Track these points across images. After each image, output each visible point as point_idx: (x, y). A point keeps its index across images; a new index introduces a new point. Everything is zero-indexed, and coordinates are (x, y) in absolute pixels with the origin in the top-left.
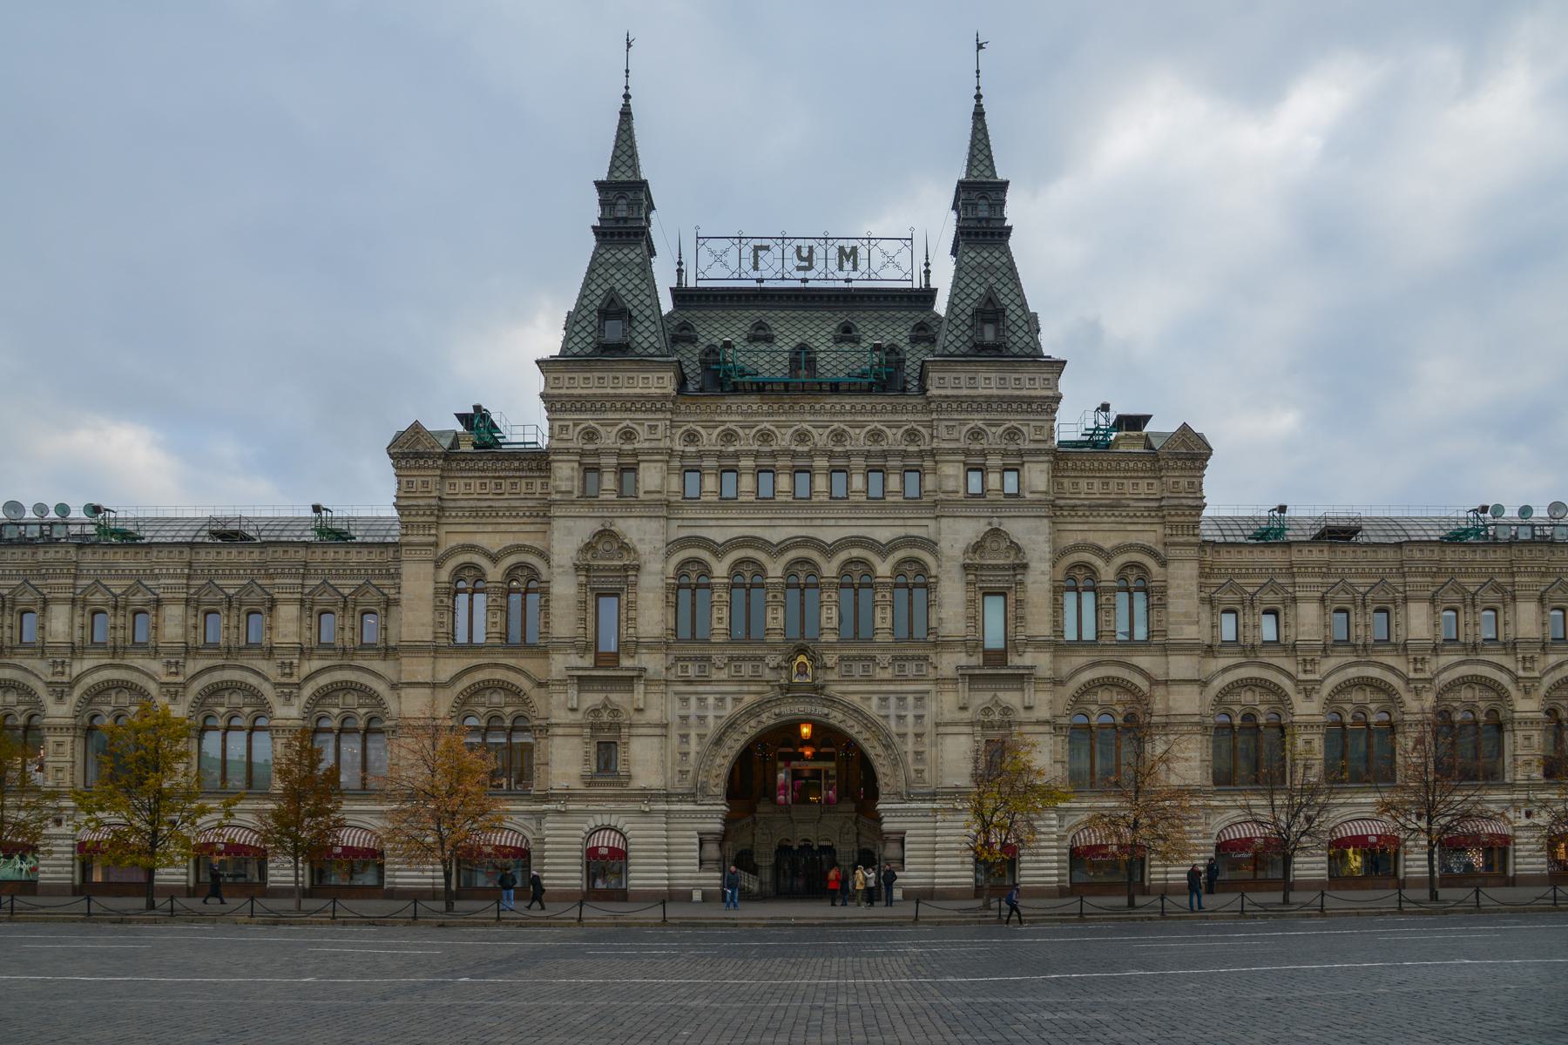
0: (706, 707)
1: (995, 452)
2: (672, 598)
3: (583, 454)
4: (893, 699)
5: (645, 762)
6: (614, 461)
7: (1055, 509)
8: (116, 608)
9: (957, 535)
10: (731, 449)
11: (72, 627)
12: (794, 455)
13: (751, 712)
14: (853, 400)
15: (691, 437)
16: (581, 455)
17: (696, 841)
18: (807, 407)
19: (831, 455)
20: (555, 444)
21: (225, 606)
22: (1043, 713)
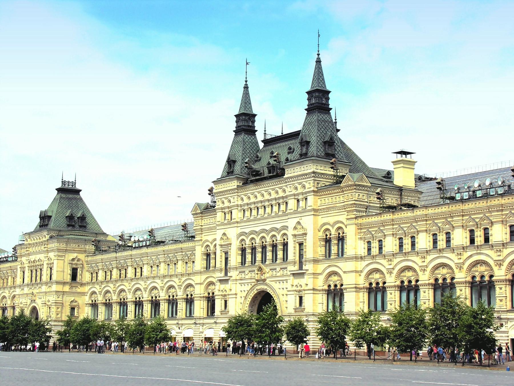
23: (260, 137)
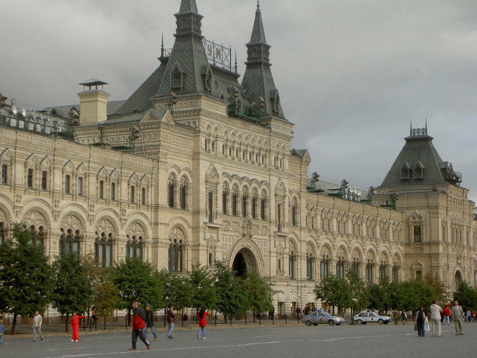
9: (274, 181)
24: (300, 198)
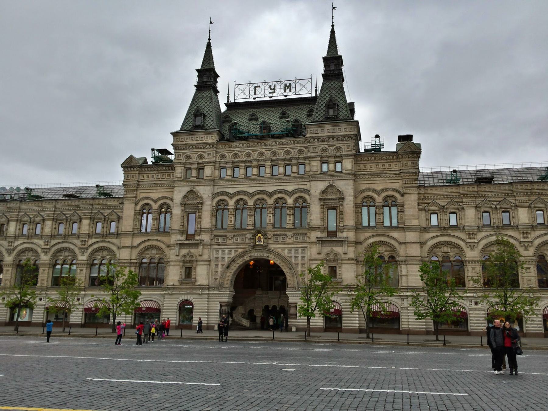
0: (225, 254)
1: (331, 156)
2: (215, 214)
3: (185, 164)
4: (293, 250)
5: (202, 274)
6: (196, 166)
7: (355, 176)
8: (30, 222)
10: (237, 160)
11: (16, 229)
12: (259, 161)
13: (241, 256)
14: (279, 140)
15: (223, 156)
16: (185, 164)
17: (219, 305)
18: (263, 144)
19: (272, 160)
20: (176, 161)
21: (65, 221)
22: (351, 255)
23: (222, 100)
24: (402, 195)
